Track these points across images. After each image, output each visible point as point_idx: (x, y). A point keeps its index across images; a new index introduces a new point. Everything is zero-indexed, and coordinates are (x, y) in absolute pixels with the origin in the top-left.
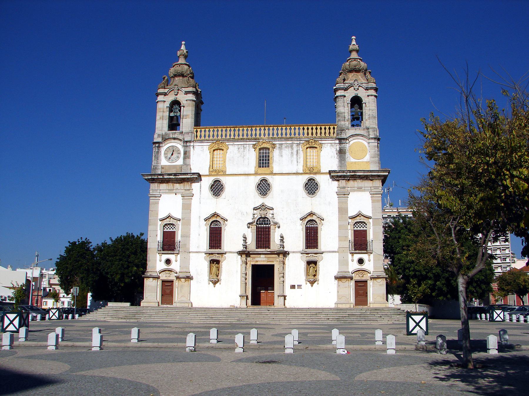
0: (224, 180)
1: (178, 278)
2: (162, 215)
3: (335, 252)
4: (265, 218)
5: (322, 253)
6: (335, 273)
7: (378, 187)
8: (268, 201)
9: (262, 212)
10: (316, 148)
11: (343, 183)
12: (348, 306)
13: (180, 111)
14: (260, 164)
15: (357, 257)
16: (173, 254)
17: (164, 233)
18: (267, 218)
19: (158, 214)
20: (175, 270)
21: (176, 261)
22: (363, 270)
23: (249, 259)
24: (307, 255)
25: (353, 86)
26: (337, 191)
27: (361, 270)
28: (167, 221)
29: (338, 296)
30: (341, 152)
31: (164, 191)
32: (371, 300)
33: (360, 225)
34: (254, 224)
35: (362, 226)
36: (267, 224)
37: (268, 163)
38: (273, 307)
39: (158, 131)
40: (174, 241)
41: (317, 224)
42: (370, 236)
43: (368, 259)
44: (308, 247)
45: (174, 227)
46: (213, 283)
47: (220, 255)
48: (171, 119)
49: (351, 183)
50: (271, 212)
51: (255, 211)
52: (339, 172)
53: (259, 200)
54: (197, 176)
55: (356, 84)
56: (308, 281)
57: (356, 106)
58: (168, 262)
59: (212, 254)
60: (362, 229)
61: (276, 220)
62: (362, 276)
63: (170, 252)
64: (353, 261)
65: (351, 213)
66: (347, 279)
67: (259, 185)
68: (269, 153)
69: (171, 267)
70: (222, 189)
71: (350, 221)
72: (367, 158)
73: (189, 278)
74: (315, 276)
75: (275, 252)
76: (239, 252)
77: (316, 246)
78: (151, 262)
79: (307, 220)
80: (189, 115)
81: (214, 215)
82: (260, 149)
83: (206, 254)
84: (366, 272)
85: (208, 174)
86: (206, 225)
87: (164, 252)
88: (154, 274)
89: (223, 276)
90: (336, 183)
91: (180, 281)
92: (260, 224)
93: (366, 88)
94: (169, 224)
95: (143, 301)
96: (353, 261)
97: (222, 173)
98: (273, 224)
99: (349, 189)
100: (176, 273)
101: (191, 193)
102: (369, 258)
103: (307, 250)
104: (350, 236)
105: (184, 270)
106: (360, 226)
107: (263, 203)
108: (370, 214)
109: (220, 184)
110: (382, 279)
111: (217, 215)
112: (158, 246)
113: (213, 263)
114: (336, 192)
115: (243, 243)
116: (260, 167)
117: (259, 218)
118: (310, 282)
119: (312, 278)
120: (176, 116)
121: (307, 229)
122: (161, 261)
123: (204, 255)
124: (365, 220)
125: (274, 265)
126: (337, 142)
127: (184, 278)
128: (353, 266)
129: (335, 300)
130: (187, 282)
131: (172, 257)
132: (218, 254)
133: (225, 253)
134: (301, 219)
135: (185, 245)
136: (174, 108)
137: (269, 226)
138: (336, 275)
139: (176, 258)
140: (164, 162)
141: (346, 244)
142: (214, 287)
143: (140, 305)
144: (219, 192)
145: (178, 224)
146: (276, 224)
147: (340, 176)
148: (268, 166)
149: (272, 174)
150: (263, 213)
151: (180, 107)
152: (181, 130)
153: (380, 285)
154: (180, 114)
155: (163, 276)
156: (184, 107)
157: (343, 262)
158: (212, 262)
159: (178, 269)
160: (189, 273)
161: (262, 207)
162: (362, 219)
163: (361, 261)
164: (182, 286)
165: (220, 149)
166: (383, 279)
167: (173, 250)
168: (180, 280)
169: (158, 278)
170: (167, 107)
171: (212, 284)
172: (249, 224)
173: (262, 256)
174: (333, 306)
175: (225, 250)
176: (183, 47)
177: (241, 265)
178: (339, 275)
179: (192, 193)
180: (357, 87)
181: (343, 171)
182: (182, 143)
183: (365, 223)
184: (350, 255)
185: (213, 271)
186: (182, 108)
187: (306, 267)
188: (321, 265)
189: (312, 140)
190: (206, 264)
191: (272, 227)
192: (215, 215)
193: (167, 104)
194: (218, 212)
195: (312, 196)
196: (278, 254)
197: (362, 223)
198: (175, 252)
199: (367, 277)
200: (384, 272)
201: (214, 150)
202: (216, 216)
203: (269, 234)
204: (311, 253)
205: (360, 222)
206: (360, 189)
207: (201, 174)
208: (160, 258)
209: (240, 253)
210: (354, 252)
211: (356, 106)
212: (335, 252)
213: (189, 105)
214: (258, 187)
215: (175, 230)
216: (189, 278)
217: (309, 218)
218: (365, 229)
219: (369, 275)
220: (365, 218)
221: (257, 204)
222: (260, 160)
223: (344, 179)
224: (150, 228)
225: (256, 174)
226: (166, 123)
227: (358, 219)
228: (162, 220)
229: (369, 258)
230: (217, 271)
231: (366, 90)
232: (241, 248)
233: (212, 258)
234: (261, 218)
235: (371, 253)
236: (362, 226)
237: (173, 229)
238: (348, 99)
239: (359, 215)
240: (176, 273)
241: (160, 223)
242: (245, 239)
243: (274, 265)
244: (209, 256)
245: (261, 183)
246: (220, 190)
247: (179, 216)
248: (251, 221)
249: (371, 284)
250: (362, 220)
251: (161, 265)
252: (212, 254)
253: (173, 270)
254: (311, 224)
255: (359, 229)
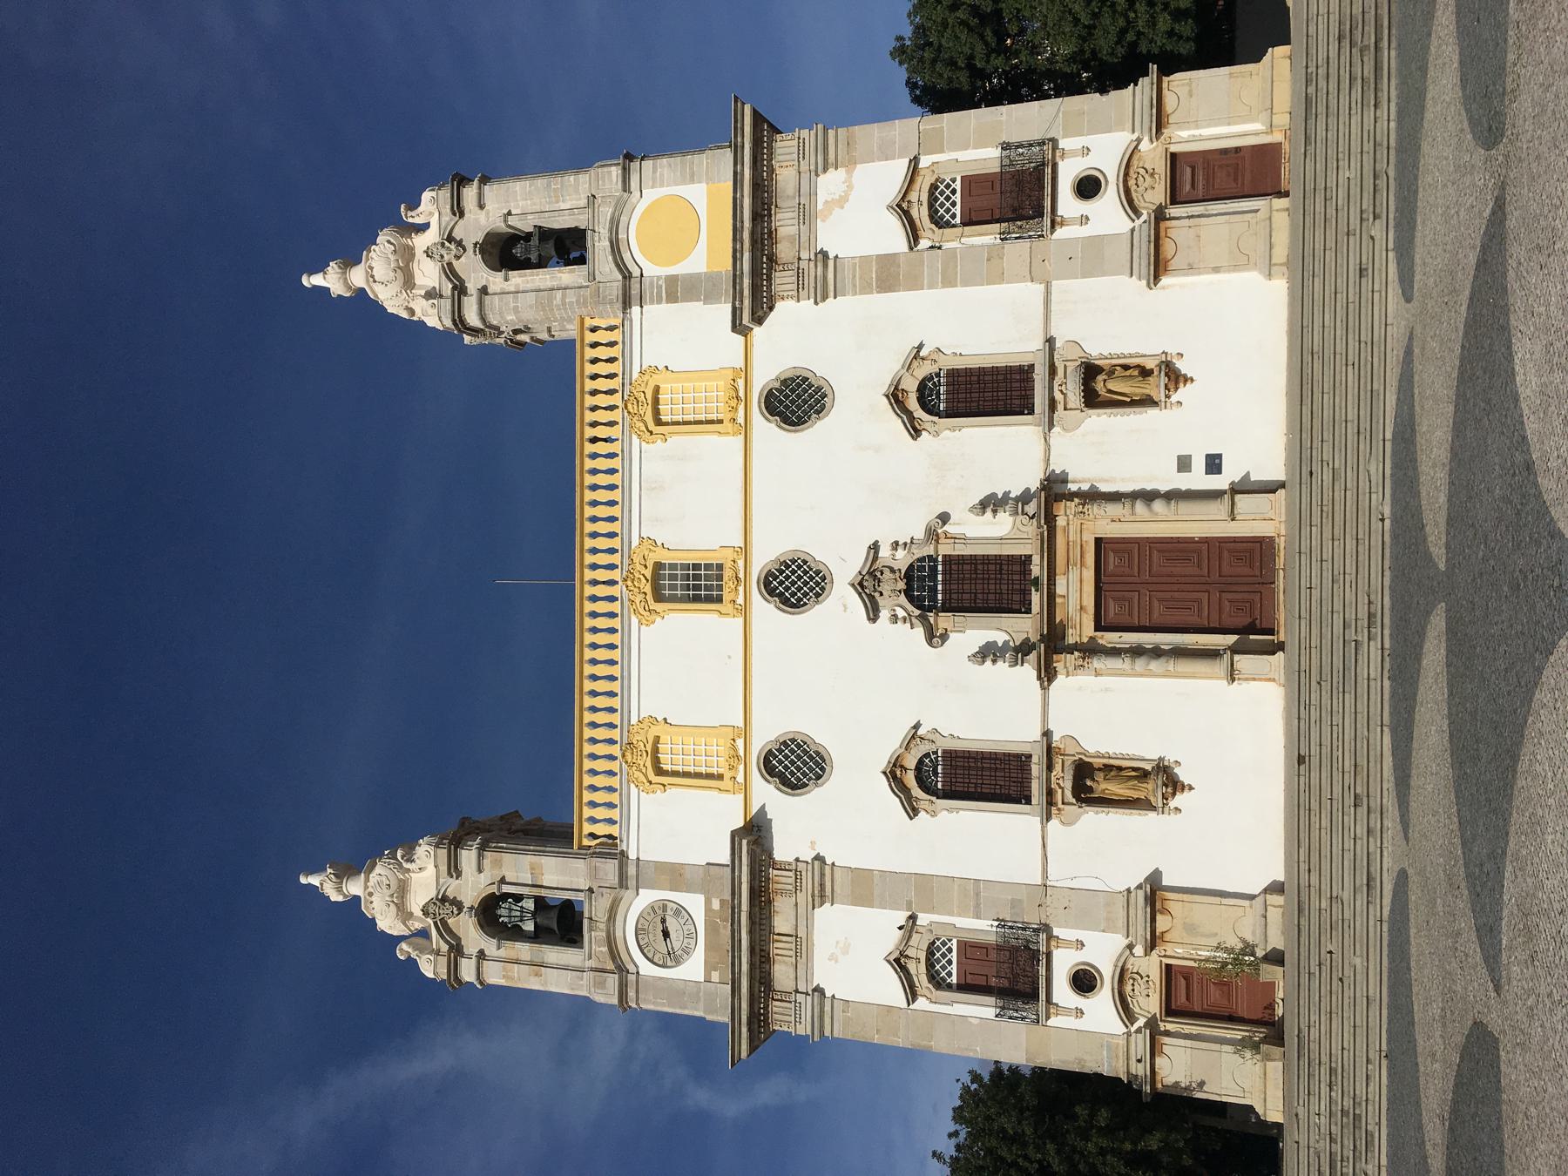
0: (764, 736)
1: (1153, 942)
2: (894, 993)
3: (1048, 293)
4: (909, 575)
5: (1050, 341)
6: (1135, 286)
7: (801, 145)
8: (844, 566)
9: (886, 588)
10: (657, 390)
11: (783, 280)
12: (1282, 222)
13: (518, 898)
14: (709, 599)
15: (1068, 203)
16: (1049, 955)
17: (963, 987)
18: (911, 566)
19: (890, 1009)
20: (1121, 955)
21: (1080, 944)
22: (1126, 174)
23: (1072, 638)
24: (1060, 407)
25: (450, 264)
26: (812, 300)
27: (1125, 182)
28: (919, 971)
29: (1236, 267)
30: (677, 290)
31: (801, 972)
32: (1258, 126)
33: (942, 205)
34: (932, 620)
35: (948, 199)
36: (934, 570)
37: (708, 567)
38: (1281, 542)
39: (582, 987)
40: (999, 948)
41: (938, 375)
42: (985, 157)
43: (1080, 158)
44: (1026, 408)
45: (944, 944)
46: (1174, 794)
47: (1058, 761)
48: (540, 936)
49: (784, 251)
50: (885, 552)
51: (884, 614)
52: (737, 295)
53: (842, 600)
54: (744, 842)
55: (443, 252)
56: (1168, 397)
57: (518, 251)
58: (1084, 982)
59: (1050, 793)
60: (957, 198)
61: (920, 534)
62: (1152, 175)
63: (1042, 971)
64: (1084, 220)
65: (893, 238)
66: (1162, 234)
67: (786, 602)
68: (673, 566)
69: (1107, 971)
70: (799, 746)
71: (924, 243)
72: (697, 193)
73: (1154, 892)
74: (1145, 373)
75: (1042, 534)
76: (1039, 678)
77: (1023, 374)
78: (1086, 1057)
79: (919, 413)
80: (531, 864)
81: (894, 777)
82: (659, 598)
83: (1049, 818)
84: (1135, 162)
85: (743, 795)
86: (934, 814)
87: (1043, 996)
88: (1141, 1044)
89: (1142, 747)
90: (779, 305)
91: (1167, 937)
92: (933, 598)
93: (455, 214)
94: (930, 965)
95: (1259, 1109)
96: (1084, 220)
97: (740, 743)
98: (932, 546)
99: (804, 255)
100: (1130, 947)
101: (810, 867)
102: (1074, 153)
103: (1037, 409)
104: (985, 237)
105: (1121, 914)
106: (948, 204)
107: (853, 585)
108: (901, 166)
109: (779, 750)
110: (1165, 91)
111: (894, 765)
112: (1017, 1018)
113: (1091, 790)
114: (816, 303)
115: (1007, 664)
116: (719, 600)
117: (911, 598)
118: (1171, 386)
119: (1155, 387)
120: (534, 914)
121: (951, 413)
122: (1079, 1012)
123: (1054, 823)
124: (923, 183)
125: (1098, 541)
126: (636, 309)
127: (1153, 920)
128: (1107, 214)
129: (1252, 278)
130: (1171, 906)
131: (1063, 963)
132: (1050, 768)
133: (1047, 734)
134: (915, 432)
135: (1014, 904)
136: (506, 920)
137: (940, 559)
138: (1144, 282)
139: (1068, 944)
140: (693, 969)
141: (1018, 250)
142: (1191, 788)
143: (1279, 1126)
144: (811, 758)
145: (930, 928)
146: (932, 535)
147: (755, 289)
148: (720, 567)
149: (745, 550)
150: (891, 587)
151: (505, 897)
152: (581, 897)
153: (1191, 96)
154: (529, 897)
155: (1149, 1003)
156: (503, 881)
157: (1092, 258)
158: (1084, 795)
159: (1118, 941)
160: (1133, 895)
161: (868, 586)
162: (920, 194)
163: (1088, 187)
164: (1191, 928)
165: (656, 750)
166: (1165, 85)
167: (1035, 956)
168: (1163, 933)
169: (1154, 1031)
170: (499, 948)
171: (1179, 796)
172: (930, 643)
173: (1060, 589)
174: (1279, 288)
175: (1035, 734)
176: (314, 880)
177: (1097, 673)
178: (1144, 271)
179: (810, 862)
180: (453, 246)
181: (736, 278)
182: (628, 894)
183: (934, 187)
184: (1060, 233)
185: (1121, 792)
186: (506, 889)
187: (1108, 411)
188: (1099, 348)
189: (630, 406)
190: (1093, 820)
191: (945, 549)
192: (894, 774)
193: (490, 946)
194: (883, 764)
195: (830, 396)
196: (1050, 519)
197: (936, 199)
198: (1043, 949)
199: (1152, 154)
200: (1136, 85)
201: (660, 771)
202: (898, 773)
203: (973, 560)
204: (1051, 389)
205: (931, 206)
206: (806, 215)
207: (739, 823)
208: (1067, 1011)
209: (1047, 675)
210: (1047, 221)
211: (518, 251)
212: (1048, 293)
213: (497, 864)
214: (793, 606)
215: (954, 941)
216: (1154, 892)
217: (913, 404)
218: (958, 185)
219: (1145, 145)
220: (916, 186)
221: (857, 606)
222: (697, 599)
223: (769, 279)
224: (941, 1043)
225: (745, 611)
226: (554, 954)
227: (921, 213)
228: (912, 993)
229: (1074, 153)
230: (1124, 773)
231: (462, 215)
232: (1027, 672)
233: (1068, 794)
234: (908, 593)
235: (1055, 147)
236: (948, 199)
237: (950, 950)
238: (496, 280)
239: (902, 210)
240: (1130, 947)
241: (921, 1003)
242: (988, 653)
243: (1098, 541)
244: (1060, 806)
245: (781, 595)
246: (805, 752)
247: (901, 917)
248: (920, 631)
249: (1184, 134)
250: (925, 197)
251: (1100, 1012)
252: (1050, 793)
253: (1120, 965)
254: (938, 394)
255: (957, 210)
